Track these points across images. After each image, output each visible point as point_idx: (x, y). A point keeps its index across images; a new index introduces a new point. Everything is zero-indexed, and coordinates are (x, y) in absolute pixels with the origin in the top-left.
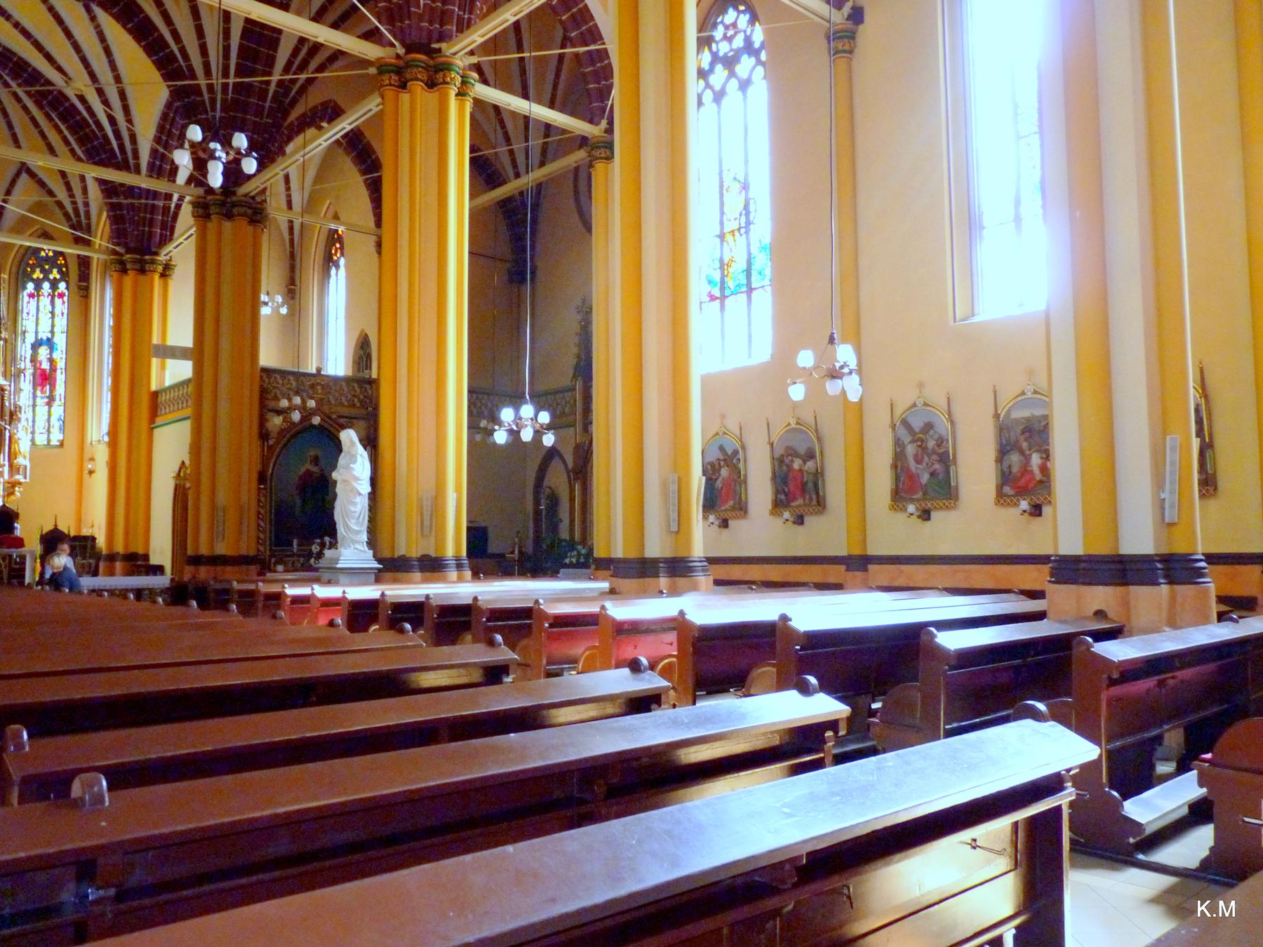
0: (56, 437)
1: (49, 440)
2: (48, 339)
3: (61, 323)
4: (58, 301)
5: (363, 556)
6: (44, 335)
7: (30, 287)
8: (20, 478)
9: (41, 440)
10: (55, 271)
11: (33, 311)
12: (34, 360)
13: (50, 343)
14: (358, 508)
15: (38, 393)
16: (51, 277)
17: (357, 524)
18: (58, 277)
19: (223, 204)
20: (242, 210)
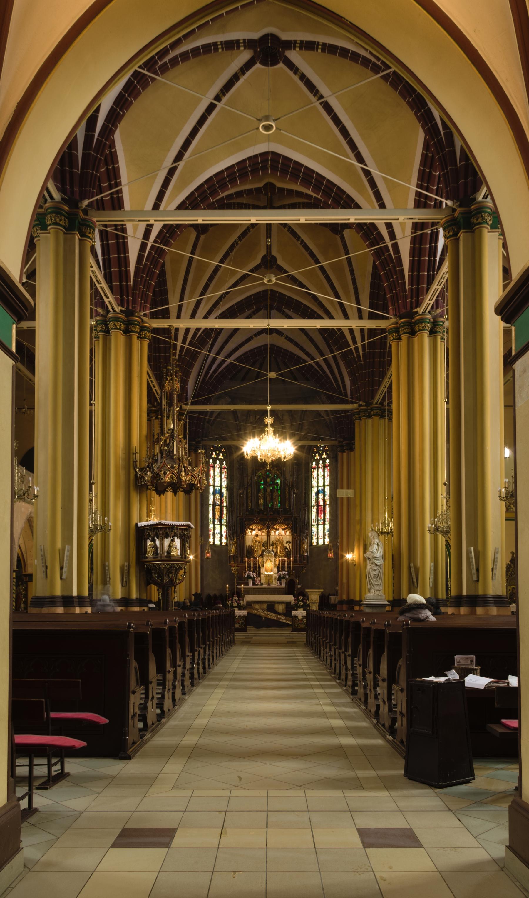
1: (324, 542)
4: (326, 469)
7: (314, 463)
9: (321, 542)
12: (317, 501)
13: (324, 491)
19: (366, 410)
20: (375, 412)
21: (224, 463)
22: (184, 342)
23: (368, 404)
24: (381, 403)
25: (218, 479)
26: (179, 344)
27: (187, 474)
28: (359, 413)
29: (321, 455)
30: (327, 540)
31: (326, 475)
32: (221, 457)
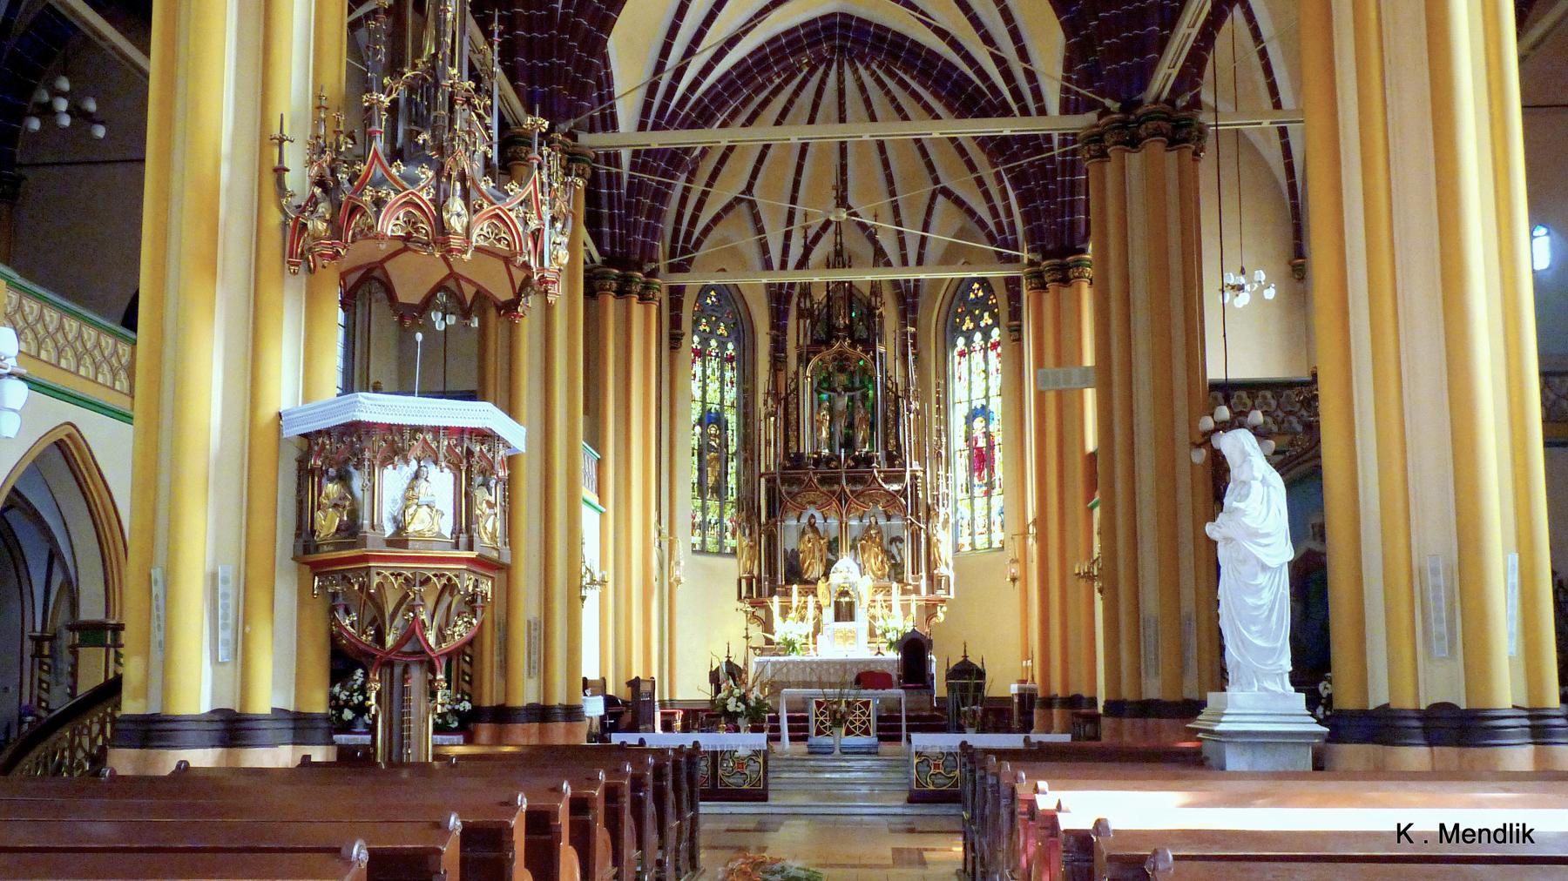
0: (998, 535)
1: (990, 544)
2: (983, 407)
3: (996, 381)
4: (992, 355)
5: (1281, 706)
6: (978, 404)
7: (961, 341)
8: (941, 593)
10: (986, 315)
11: (965, 374)
12: (969, 438)
13: (984, 412)
14: (1266, 597)
15: (976, 481)
16: (982, 324)
17: (1261, 634)
18: (990, 322)
19: (1124, 124)
20: (1151, 125)
21: (730, 346)
23: (1129, 106)
24: (1171, 101)
25: (713, 387)
27: (472, 209)
28: (1096, 139)
31: (992, 368)
32: (722, 330)
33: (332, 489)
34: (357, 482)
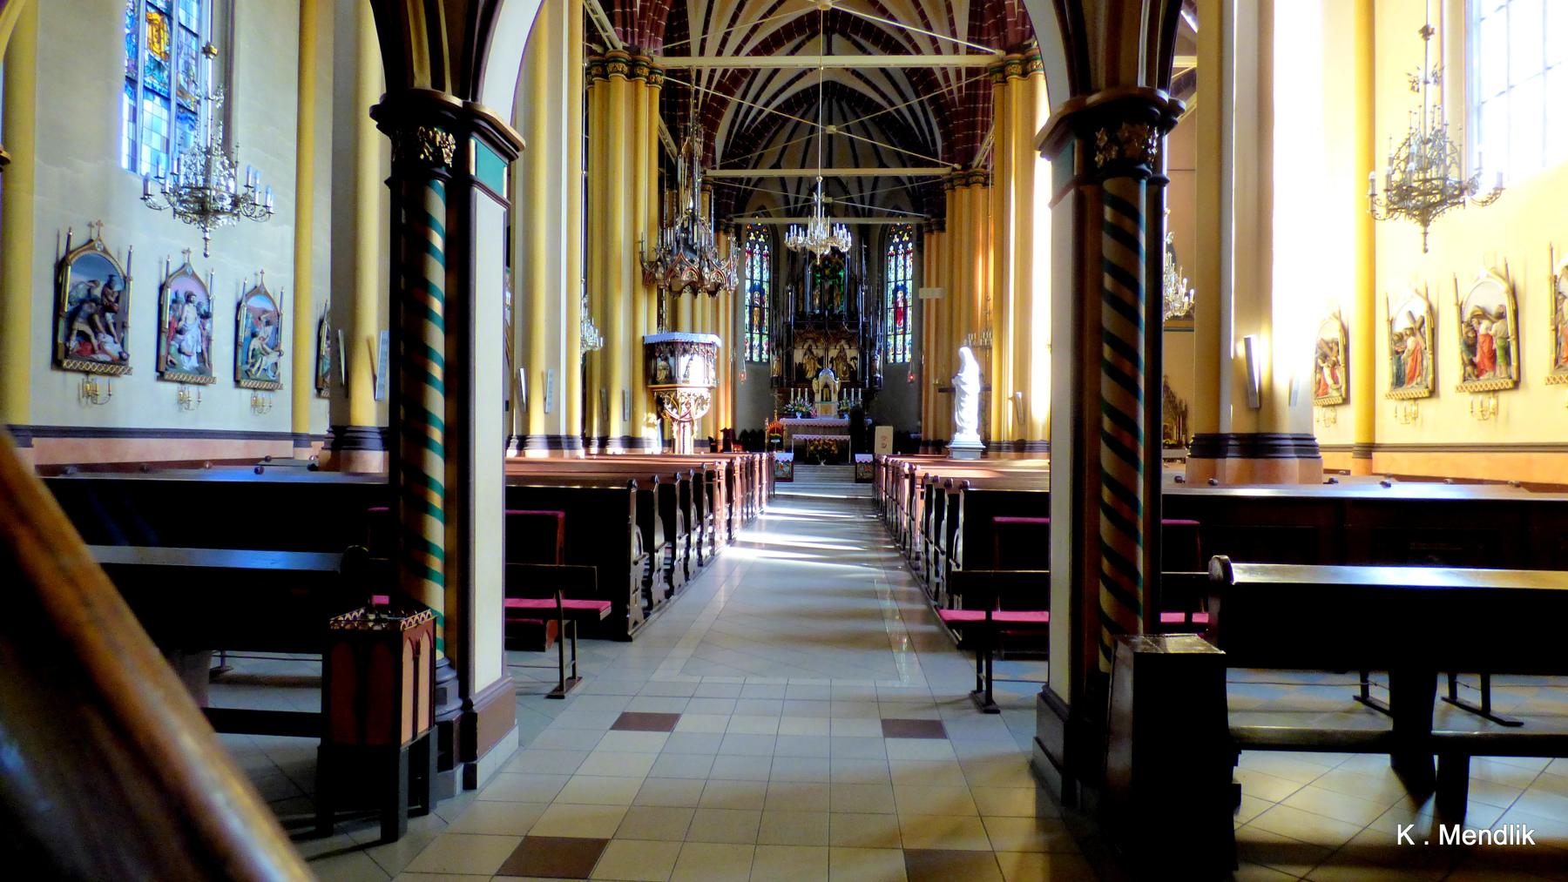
9: (899, 358)
12: (895, 302)
13: (904, 288)
22: (708, 87)
23: (966, 167)
26: (702, 89)
28: (951, 180)
29: (900, 237)
30: (908, 356)
32: (761, 239)
33: (661, 363)
34: (671, 360)
